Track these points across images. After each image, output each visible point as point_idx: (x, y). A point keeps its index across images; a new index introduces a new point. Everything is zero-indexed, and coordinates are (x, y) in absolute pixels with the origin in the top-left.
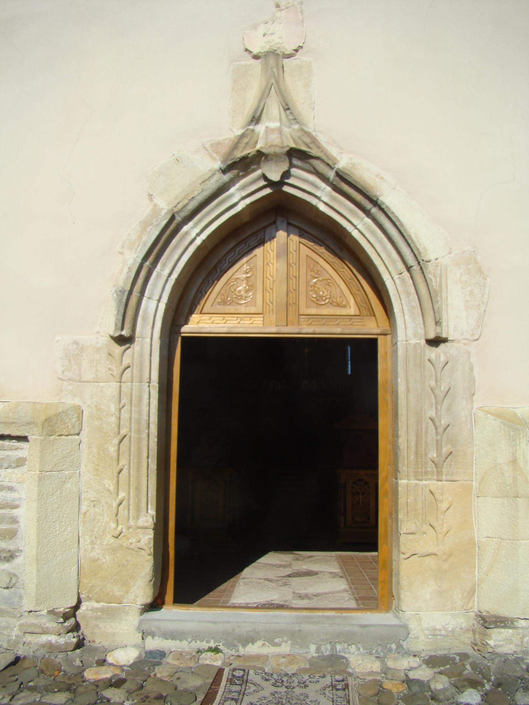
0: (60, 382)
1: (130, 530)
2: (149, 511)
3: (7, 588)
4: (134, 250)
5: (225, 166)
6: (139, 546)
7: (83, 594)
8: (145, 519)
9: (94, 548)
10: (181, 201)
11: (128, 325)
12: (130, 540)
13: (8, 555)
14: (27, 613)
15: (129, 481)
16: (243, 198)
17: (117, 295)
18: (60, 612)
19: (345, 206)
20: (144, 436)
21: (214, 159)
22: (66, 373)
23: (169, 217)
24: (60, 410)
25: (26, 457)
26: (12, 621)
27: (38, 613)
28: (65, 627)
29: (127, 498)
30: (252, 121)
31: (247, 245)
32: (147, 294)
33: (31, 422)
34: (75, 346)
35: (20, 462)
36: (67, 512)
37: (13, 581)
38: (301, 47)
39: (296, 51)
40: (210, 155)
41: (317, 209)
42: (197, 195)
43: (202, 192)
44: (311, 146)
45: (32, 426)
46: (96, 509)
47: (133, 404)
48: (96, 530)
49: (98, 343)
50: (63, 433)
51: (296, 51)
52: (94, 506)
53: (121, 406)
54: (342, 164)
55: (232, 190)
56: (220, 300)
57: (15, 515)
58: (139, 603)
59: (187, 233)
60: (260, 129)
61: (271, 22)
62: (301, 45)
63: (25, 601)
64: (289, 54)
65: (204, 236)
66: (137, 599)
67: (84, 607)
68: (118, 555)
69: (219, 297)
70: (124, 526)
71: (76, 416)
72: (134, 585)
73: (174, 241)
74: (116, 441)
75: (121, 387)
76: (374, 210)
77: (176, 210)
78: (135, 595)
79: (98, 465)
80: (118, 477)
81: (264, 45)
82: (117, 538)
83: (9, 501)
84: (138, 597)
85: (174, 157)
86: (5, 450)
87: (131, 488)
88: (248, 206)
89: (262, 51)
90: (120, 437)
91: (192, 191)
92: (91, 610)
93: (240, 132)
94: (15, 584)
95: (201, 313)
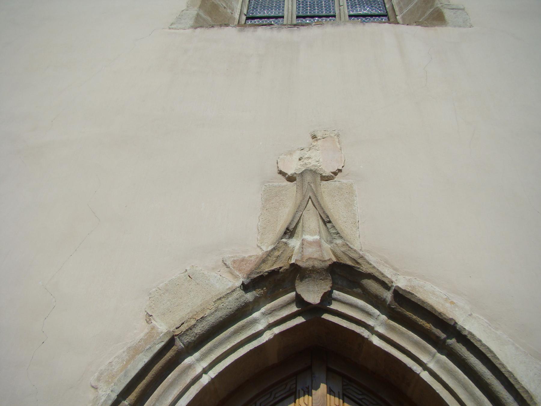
4: (113, 384)
5: (248, 281)
10: (187, 321)
16: (270, 327)
19: (408, 339)
21: (236, 277)
23: (166, 339)
30: (285, 233)
31: (273, 397)
38: (340, 171)
39: (335, 174)
40: (232, 273)
41: (370, 343)
42: (209, 315)
43: (216, 311)
44: (359, 261)
51: (335, 174)
54: (401, 282)
55: (256, 315)
59: (190, 367)
60: (295, 243)
61: (308, 149)
62: (340, 168)
64: (328, 176)
65: (213, 373)
73: (171, 377)
76: (452, 342)
77: (178, 332)
81: (299, 167)
85: (187, 273)
88: (276, 336)
89: (297, 173)
91: (203, 310)
93: (270, 248)
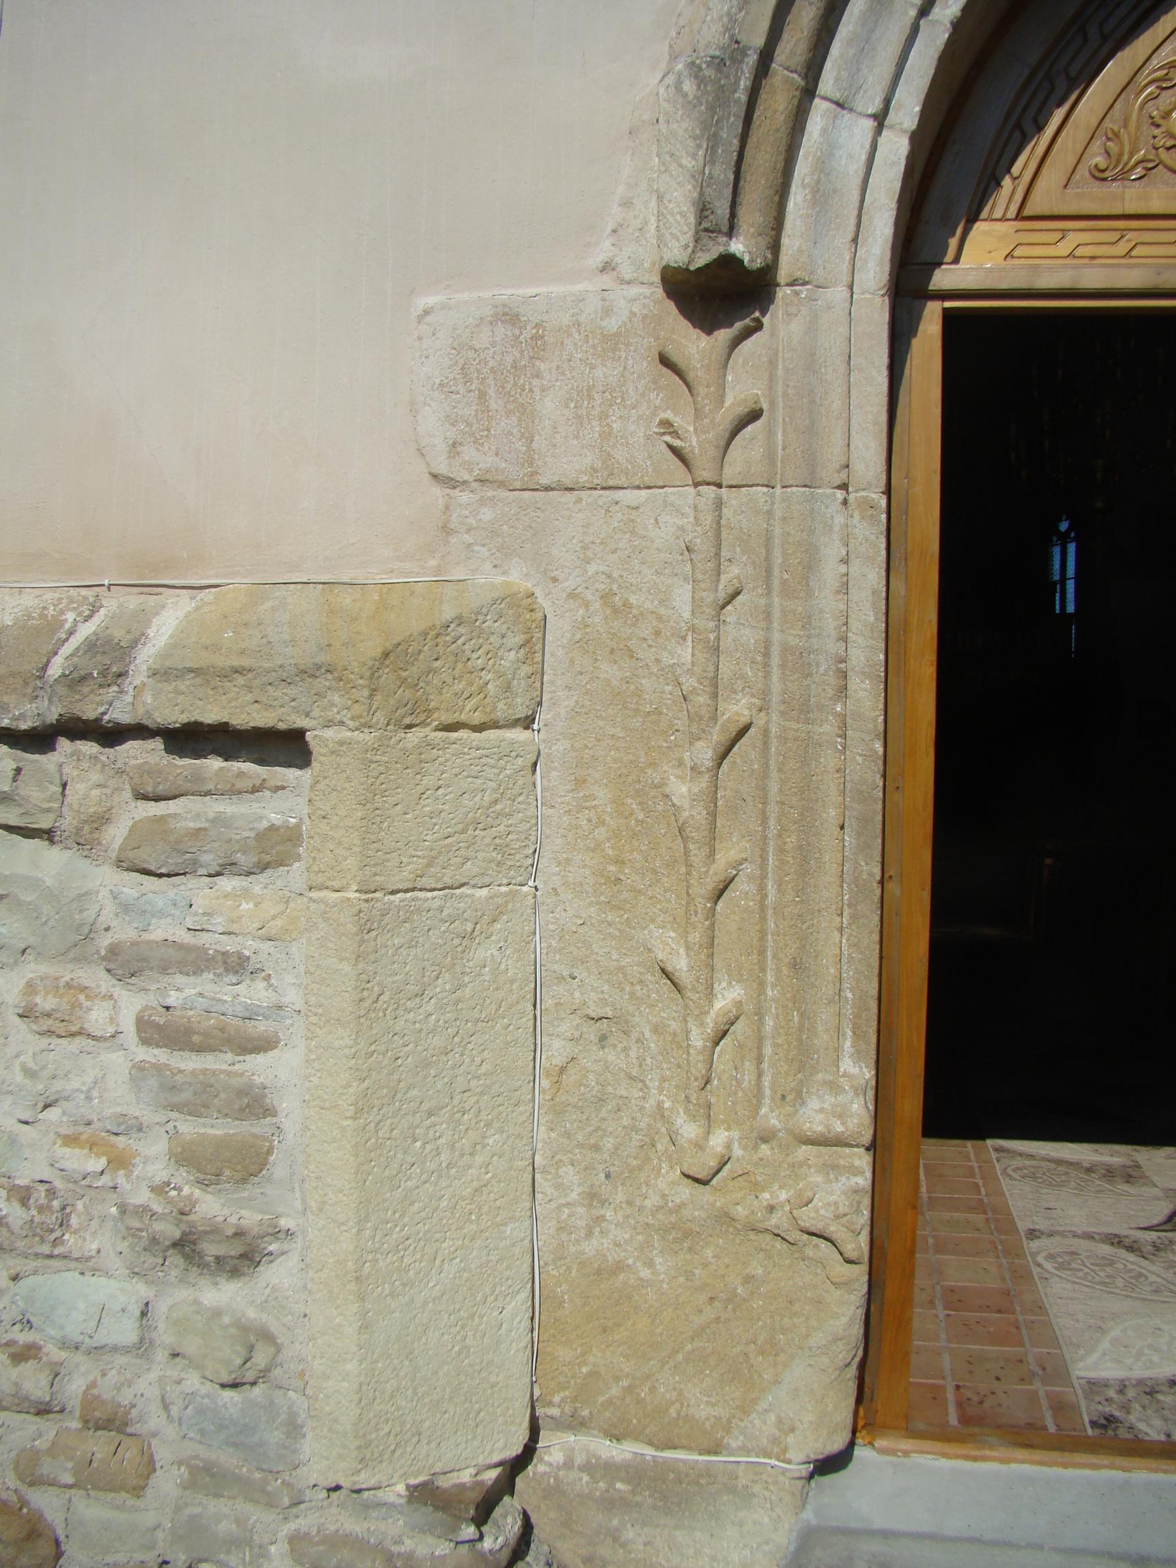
0: (438, 492)
1: (765, 1149)
2: (847, 1065)
3: (235, 1385)
6: (807, 1224)
7: (550, 1404)
8: (829, 1100)
9: (600, 1219)
11: (752, 217)
12: (766, 1195)
13: (235, 1249)
14: (324, 1494)
15: (763, 934)
17: (700, 81)
18: (461, 1487)
20: (828, 728)
22: (469, 453)
24: (448, 612)
25: (298, 826)
26: (259, 1516)
27: (366, 1494)
28: (482, 1555)
29: (749, 1007)
32: (827, 84)
33: (319, 667)
34: (501, 330)
35: (272, 851)
36: (483, 1069)
37: (260, 1359)
45: (323, 682)
46: (611, 1056)
47: (776, 584)
48: (609, 1143)
49: (608, 311)
50: (463, 717)
52: (603, 1038)
53: (722, 595)
56: (1100, 160)
57: (258, 1080)
58: (796, 1455)
63: (309, 1446)
66: (791, 1439)
67: (555, 1449)
68: (709, 1253)
69: (1097, 145)
70: (736, 1134)
71: (519, 639)
72: (777, 1382)
74: (705, 753)
75: (719, 504)
78: (780, 1420)
79: (619, 862)
80: (712, 913)
82: (705, 1183)
83: (228, 1019)
84: (793, 1430)
86: (208, 793)
87: (770, 963)
90: (717, 736)
92: (587, 1467)
94: (268, 1370)
95: (1019, 217)
